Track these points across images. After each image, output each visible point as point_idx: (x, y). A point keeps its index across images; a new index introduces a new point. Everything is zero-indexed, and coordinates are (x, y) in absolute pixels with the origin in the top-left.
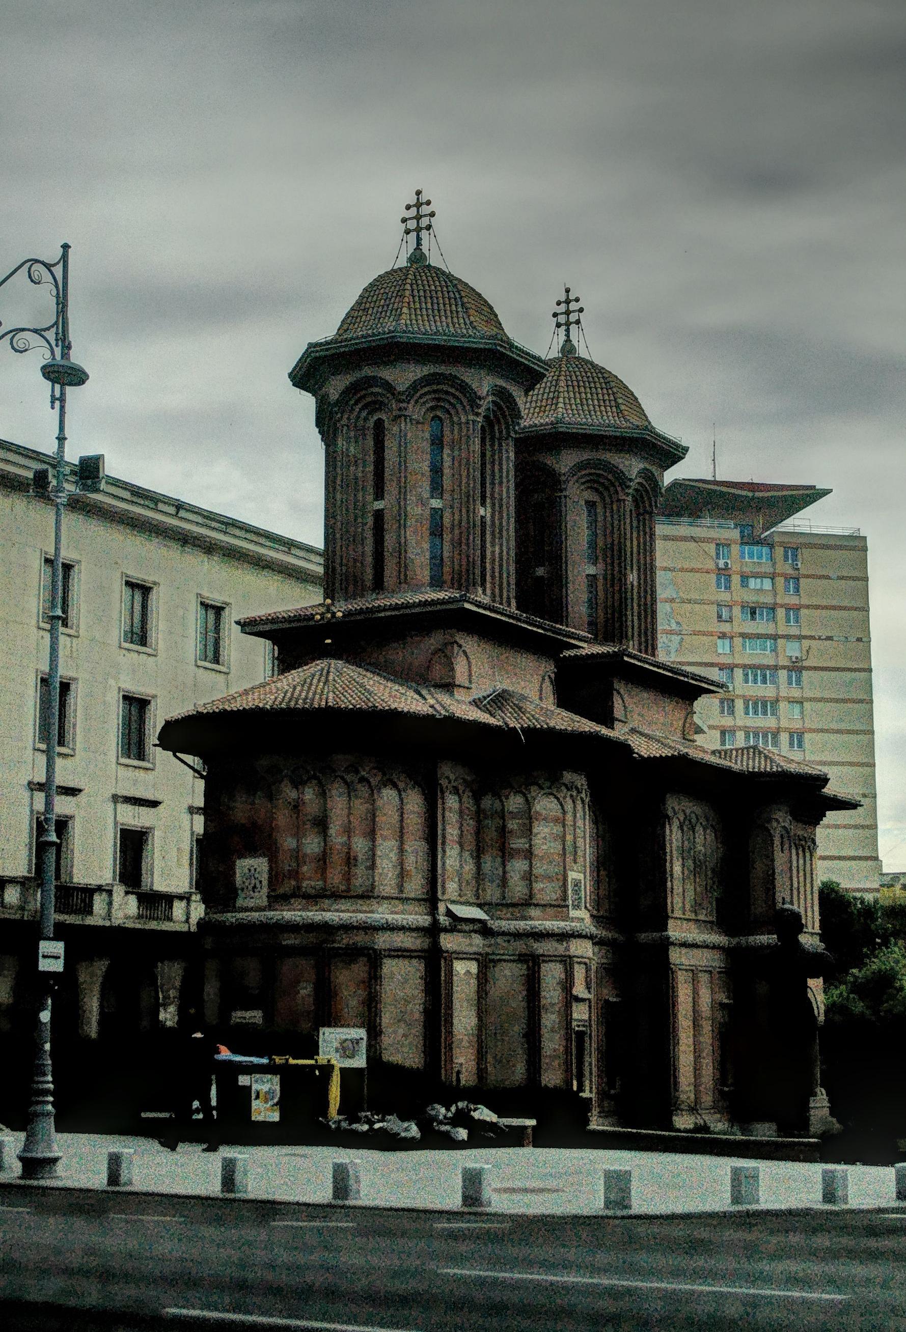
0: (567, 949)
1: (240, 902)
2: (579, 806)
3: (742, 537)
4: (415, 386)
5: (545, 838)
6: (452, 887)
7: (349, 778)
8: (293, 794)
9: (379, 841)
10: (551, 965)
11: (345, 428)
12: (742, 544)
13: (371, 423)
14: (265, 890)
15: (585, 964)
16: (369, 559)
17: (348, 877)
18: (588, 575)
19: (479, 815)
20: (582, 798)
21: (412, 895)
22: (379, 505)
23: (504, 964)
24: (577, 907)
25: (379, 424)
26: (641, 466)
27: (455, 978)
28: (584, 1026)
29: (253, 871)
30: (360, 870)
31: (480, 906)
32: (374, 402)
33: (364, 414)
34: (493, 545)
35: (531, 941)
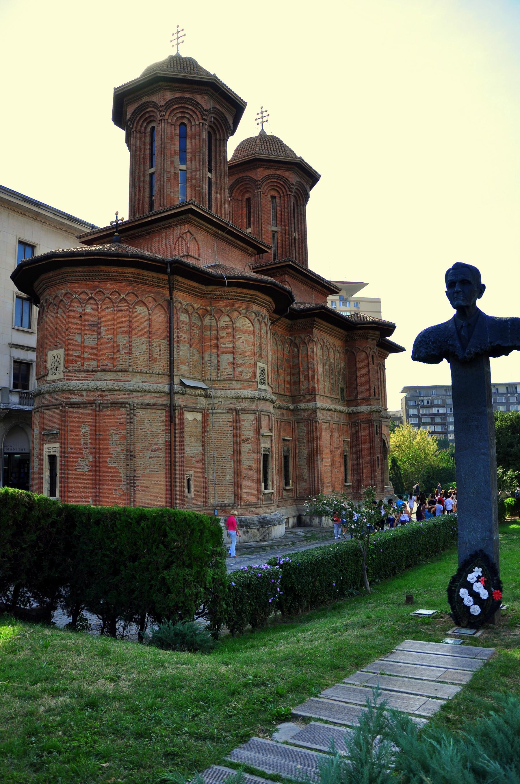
0: (257, 406)
1: (50, 378)
2: (263, 327)
3: (340, 299)
4: (169, 104)
5: (243, 342)
6: (184, 369)
7: (114, 298)
8: (80, 310)
9: (134, 337)
10: (246, 415)
12: (340, 301)
13: (149, 129)
14: (62, 368)
15: (269, 416)
16: (147, 200)
17: (113, 360)
18: (272, 231)
19: (203, 328)
20: (265, 322)
21: (157, 371)
22: (152, 170)
23: (218, 415)
24: (263, 383)
25: (153, 128)
26: (298, 180)
27: (185, 423)
28: (268, 451)
29: (56, 357)
30: (121, 355)
31: (203, 381)
32: (150, 116)
33: (145, 125)
34: (216, 193)
35: (234, 401)
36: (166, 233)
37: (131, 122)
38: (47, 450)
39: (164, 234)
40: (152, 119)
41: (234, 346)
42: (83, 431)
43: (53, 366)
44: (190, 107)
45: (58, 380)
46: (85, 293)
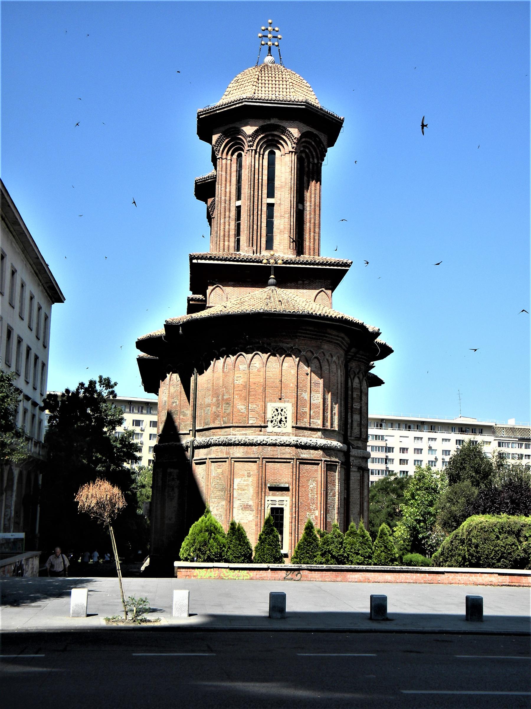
1: (270, 429)
7: (330, 358)
11: (254, 151)
14: (290, 423)
22: (270, 201)
29: (279, 411)
36: (303, 281)
37: (253, 138)
38: (270, 502)
39: (300, 282)
40: (274, 143)
41: (361, 407)
42: (311, 486)
43: (275, 418)
44: (313, 143)
45: (284, 434)
46: (311, 351)
